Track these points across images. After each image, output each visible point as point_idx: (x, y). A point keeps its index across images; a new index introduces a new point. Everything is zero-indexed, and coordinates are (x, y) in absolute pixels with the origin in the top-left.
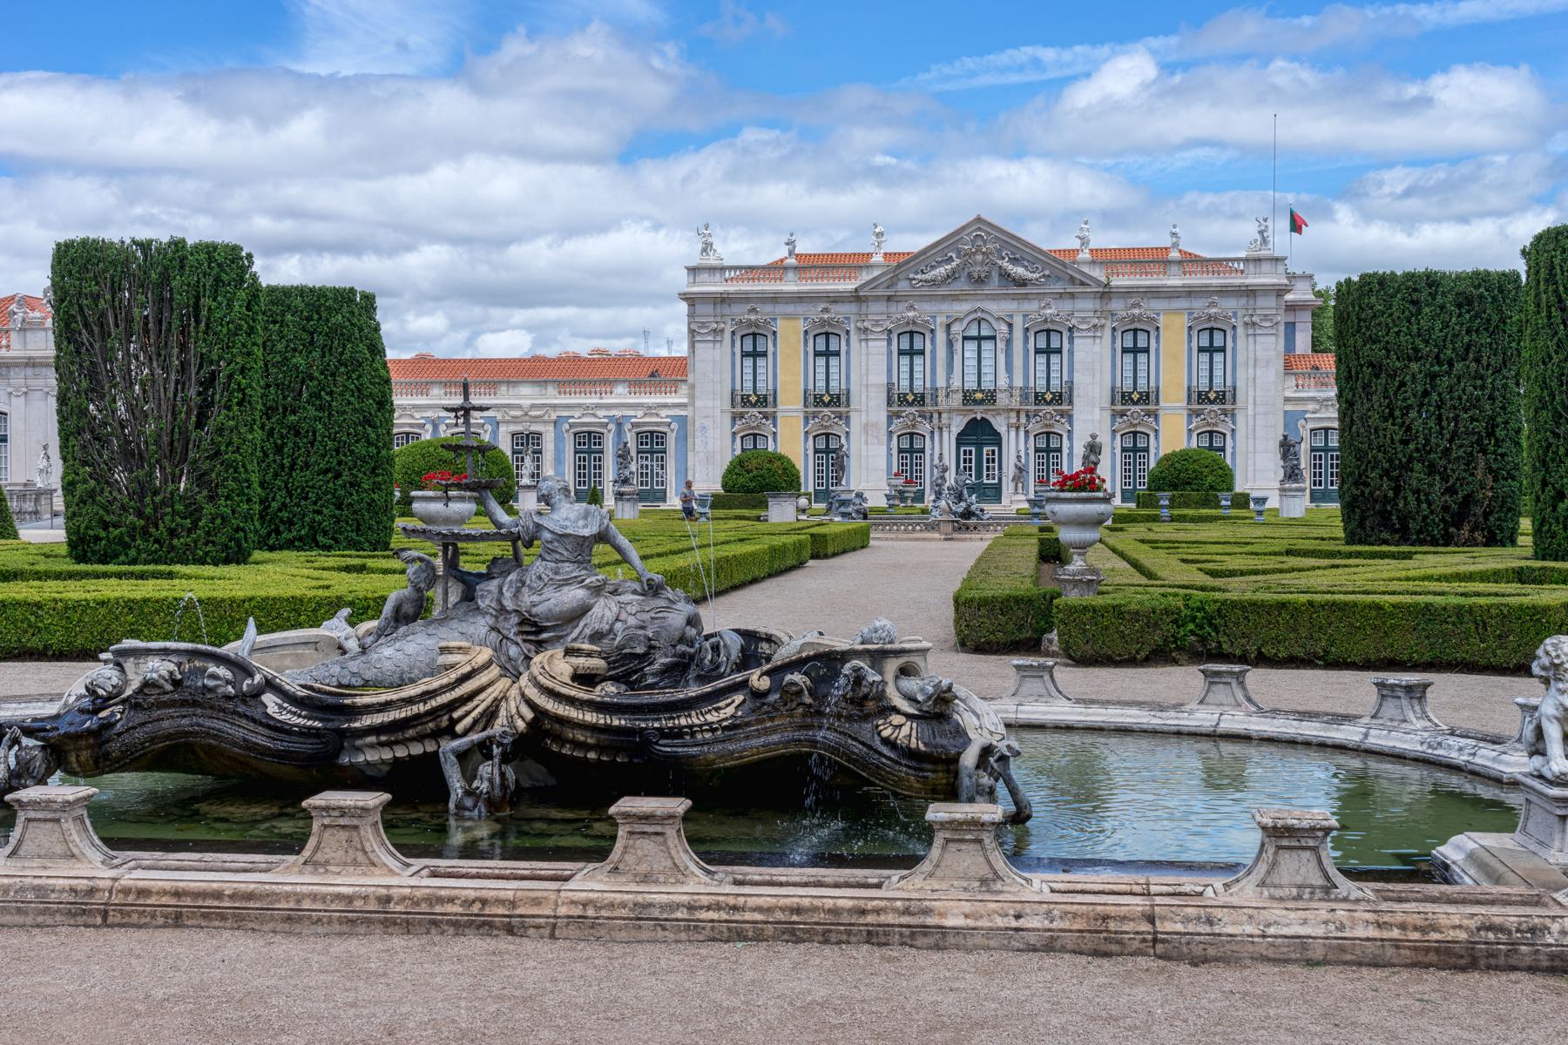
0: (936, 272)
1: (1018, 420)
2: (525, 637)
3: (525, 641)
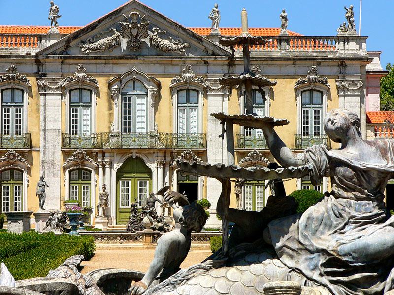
0: (101, 42)
1: (165, 159)
2: (331, 278)
3: (332, 282)
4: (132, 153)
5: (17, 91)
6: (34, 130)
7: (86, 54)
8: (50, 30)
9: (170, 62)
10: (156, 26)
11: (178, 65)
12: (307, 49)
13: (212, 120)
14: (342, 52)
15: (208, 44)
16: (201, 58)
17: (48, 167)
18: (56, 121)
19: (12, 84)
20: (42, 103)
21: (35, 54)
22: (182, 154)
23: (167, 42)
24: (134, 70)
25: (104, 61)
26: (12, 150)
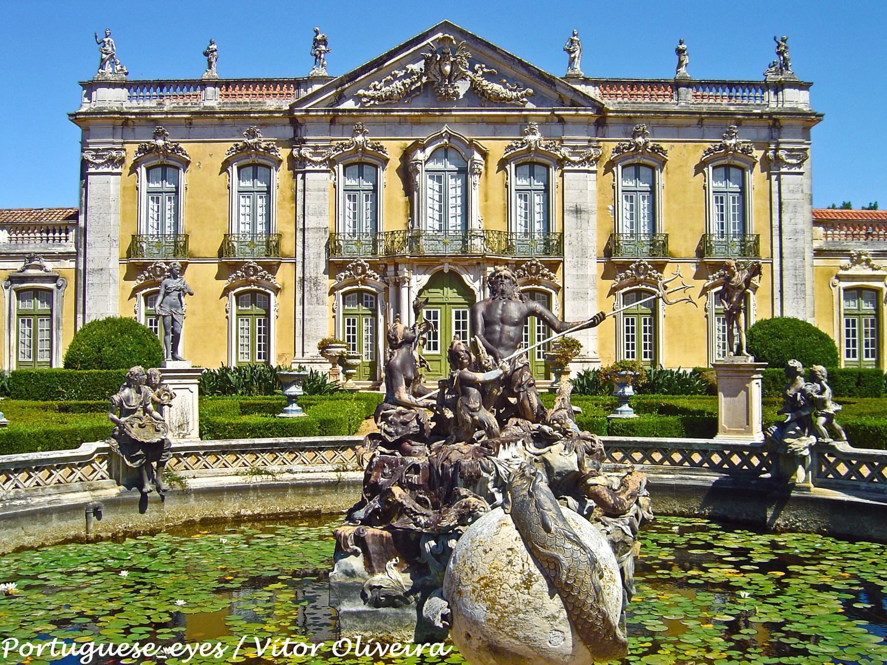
4: (443, 264)
5: (263, 168)
6: (287, 230)
7: (368, 107)
8: (314, 71)
9: (503, 119)
10: (481, 63)
11: (515, 124)
12: (719, 101)
13: (572, 211)
14: (773, 105)
15: (563, 88)
16: (553, 111)
17: (308, 289)
18: (321, 214)
19: (253, 156)
20: (300, 187)
21: (288, 108)
22: (524, 266)
23: (497, 87)
24: (446, 131)
25: (398, 119)
26: (251, 261)
